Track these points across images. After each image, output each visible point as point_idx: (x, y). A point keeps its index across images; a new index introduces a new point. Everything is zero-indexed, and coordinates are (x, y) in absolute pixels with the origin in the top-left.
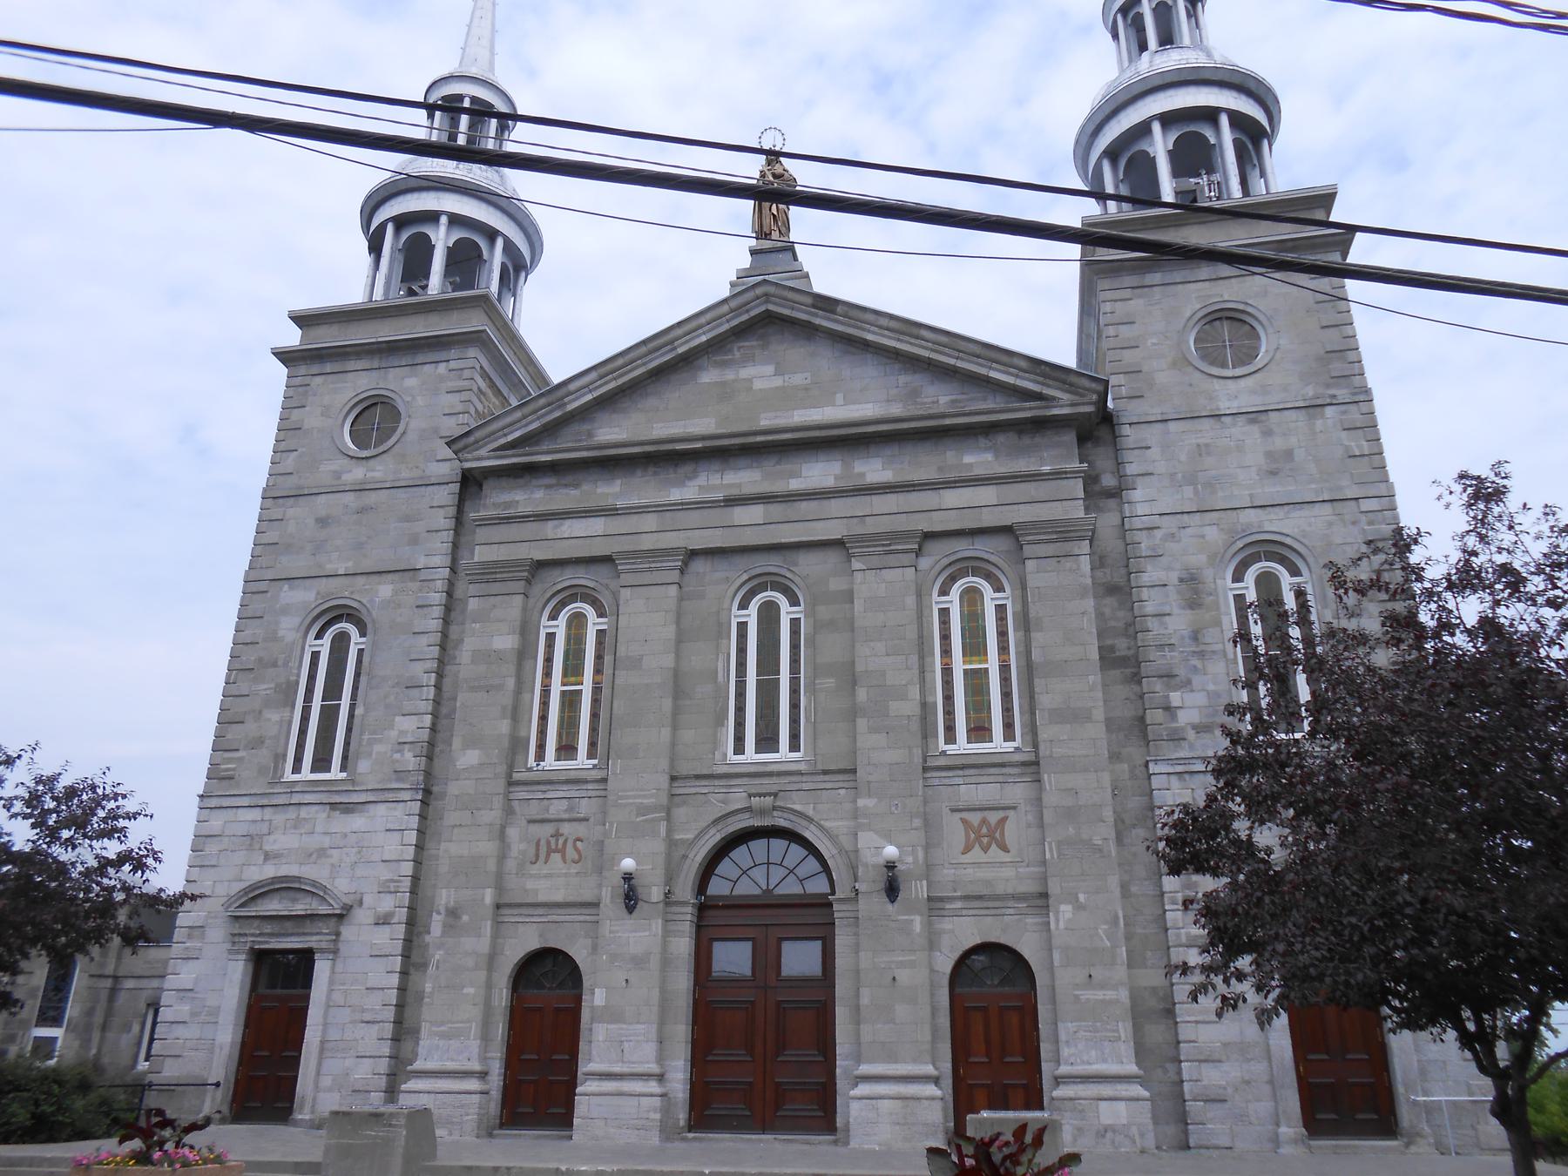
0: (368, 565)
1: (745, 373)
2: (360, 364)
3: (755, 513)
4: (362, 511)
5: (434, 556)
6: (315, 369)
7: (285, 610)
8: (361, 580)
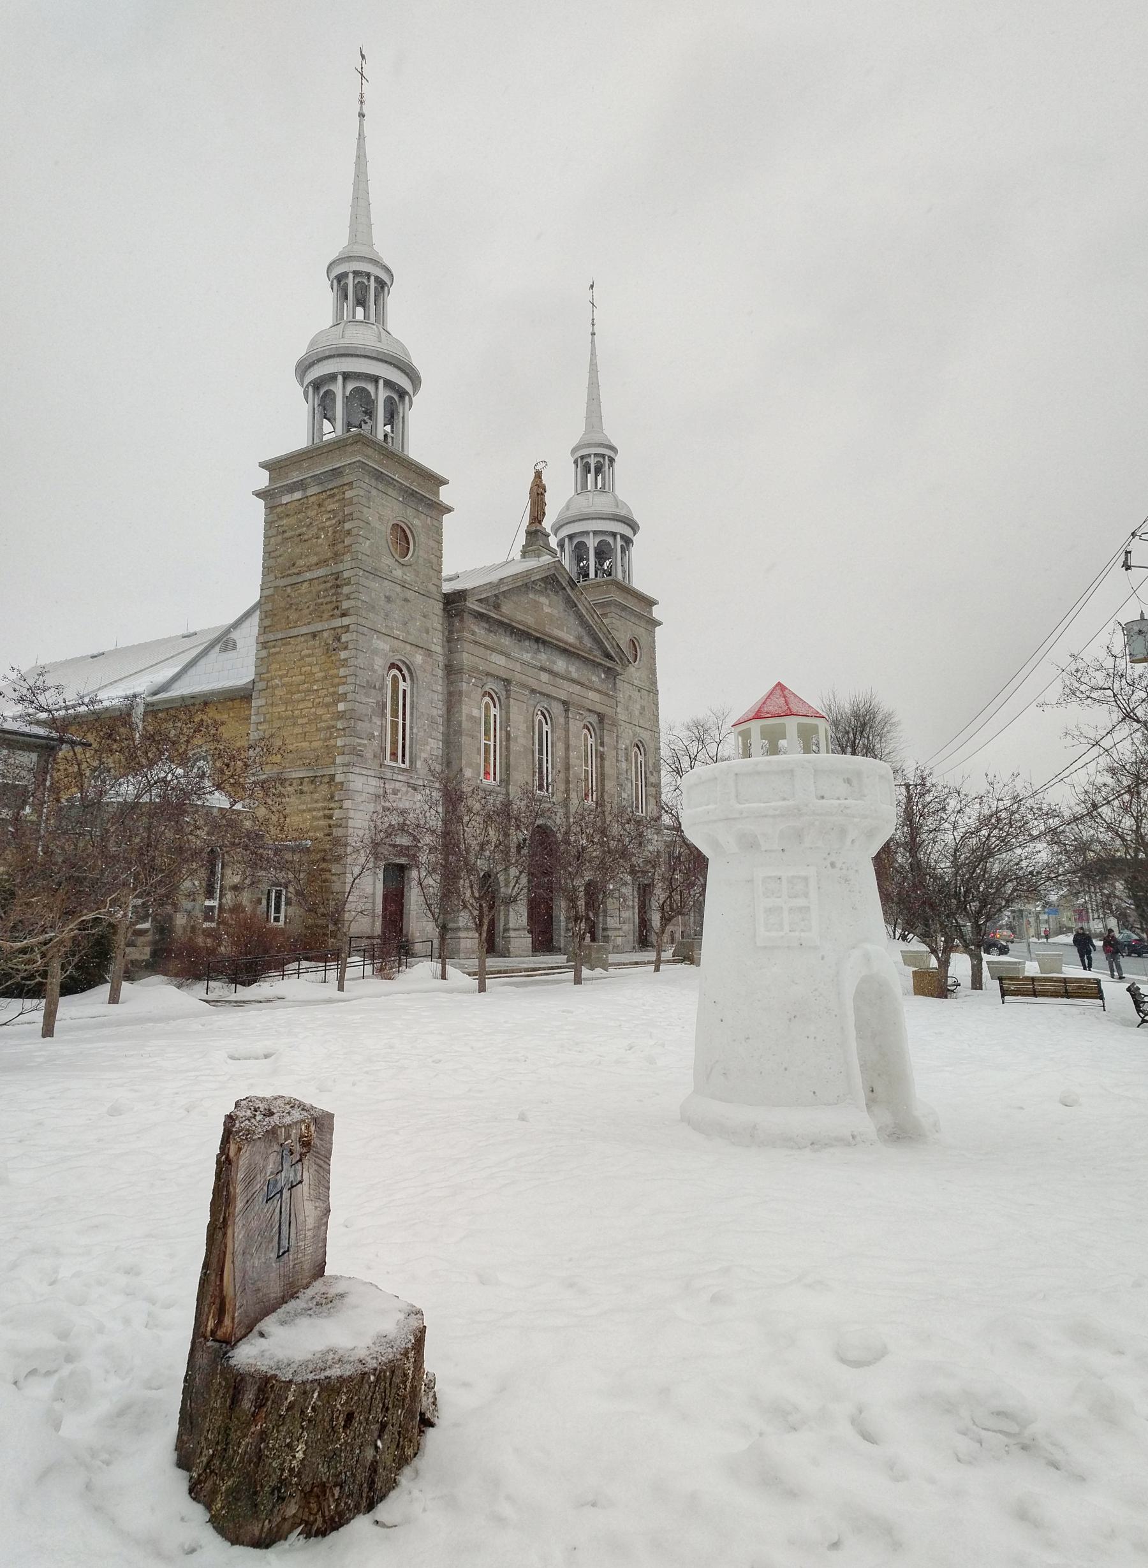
0: (411, 639)
1: (543, 600)
2: (394, 494)
3: (545, 677)
4: (406, 600)
5: (437, 646)
6: (373, 482)
7: (375, 652)
8: (408, 647)
